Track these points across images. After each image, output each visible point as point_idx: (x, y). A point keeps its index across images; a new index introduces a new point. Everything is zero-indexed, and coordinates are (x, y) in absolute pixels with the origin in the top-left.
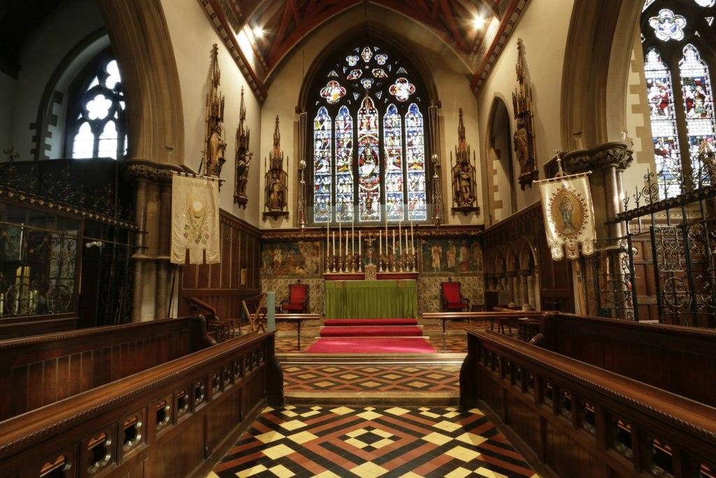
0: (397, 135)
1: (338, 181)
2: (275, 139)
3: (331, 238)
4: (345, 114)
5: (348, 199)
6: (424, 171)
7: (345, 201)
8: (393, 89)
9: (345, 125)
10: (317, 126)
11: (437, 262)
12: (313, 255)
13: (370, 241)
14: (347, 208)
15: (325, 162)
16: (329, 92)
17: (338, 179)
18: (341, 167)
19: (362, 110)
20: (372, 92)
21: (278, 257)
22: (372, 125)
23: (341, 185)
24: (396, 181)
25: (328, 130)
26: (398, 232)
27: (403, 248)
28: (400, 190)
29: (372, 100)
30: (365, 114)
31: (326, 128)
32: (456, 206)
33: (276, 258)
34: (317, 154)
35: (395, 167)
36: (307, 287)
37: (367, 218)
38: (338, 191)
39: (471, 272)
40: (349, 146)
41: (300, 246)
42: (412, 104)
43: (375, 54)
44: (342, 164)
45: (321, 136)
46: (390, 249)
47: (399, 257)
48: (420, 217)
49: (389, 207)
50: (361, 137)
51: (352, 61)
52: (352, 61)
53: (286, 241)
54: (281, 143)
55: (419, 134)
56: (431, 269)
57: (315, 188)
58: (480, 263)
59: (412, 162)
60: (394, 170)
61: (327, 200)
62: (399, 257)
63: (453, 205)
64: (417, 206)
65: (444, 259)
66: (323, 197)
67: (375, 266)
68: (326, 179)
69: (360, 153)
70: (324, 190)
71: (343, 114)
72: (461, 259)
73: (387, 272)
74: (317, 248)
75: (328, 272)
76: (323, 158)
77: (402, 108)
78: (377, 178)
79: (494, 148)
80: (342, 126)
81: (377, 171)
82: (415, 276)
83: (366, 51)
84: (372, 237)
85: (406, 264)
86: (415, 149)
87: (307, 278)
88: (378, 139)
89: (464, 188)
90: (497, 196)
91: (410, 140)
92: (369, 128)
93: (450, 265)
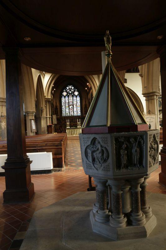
20: (71, 94)
52: (68, 88)
77: (76, 97)
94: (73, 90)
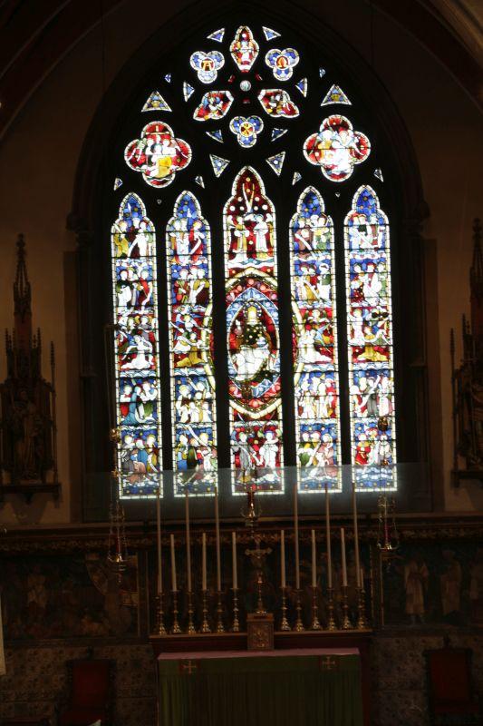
0: (324, 271)
1: (177, 391)
2: (16, 298)
3: (166, 548)
4: (189, 215)
5: (204, 438)
6: (391, 365)
7: (195, 443)
8: (314, 148)
9: (192, 243)
10: (119, 248)
14: (200, 461)
15: (141, 344)
16: (148, 152)
17: (177, 386)
18: (183, 356)
19: (234, 203)
20: (257, 155)
22: (261, 244)
23: (185, 401)
24: (322, 392)
26: (324, 531)
28: (333, 416)
29: (258, 177)
30: (241, 214)
31: (142, 252)
32: (462, 466)
33: (32, 597)
38: (178, 418)
40: (202, 299)
41: (89, 567)
42: (361, 189)
43: (265, 46)
44: (185, 349)
45: (131, 272)
46: (306, 570)
47: (323, 592)
48: (381, 483)
50: (232, 276)
51: (206, 66)
52: (206, 66)
54: (35, 307)
55: (381, 268)
60: (317, 363)
61: (151, 441)
63: (456, 464)
64: (373, 457)
68: (146, 386)
69: (231, 318)
70: (141, 415)
71: (185, 214)
76: (137, 332)
77: (338, 201)
78: (275, 385)
80: (183, 247)
81: (274, 365)
83: (241, 39)
84: (264, 545)
86: (369, 308)
88: (275, 283)
91: (356, 285)
92: (252, 252)
94: (282, 105)
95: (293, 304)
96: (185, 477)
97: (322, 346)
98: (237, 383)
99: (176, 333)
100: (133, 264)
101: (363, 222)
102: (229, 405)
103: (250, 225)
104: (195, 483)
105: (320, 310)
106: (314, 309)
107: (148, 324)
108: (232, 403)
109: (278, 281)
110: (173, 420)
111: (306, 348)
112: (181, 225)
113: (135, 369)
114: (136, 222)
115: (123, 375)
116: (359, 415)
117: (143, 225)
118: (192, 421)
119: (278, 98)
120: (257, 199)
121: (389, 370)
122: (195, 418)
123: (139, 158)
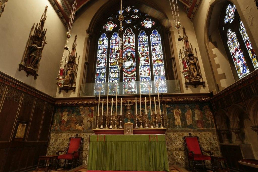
1: (110, 71)
3: (101, 104)
4: (116, 36)
5: (116, 81)
8: (143, 24)
9: (116, 41)
11: (178, 121)
12: (89, 116)
13: (129, 105)
16: (108, 26)
18: (112, 63)
19: (126, 34)
21: (65, 118)
22: (131, 41)
24: (146, 70)
25: (106, 44)
26: (149, 99)
27: (152, 111)
28: (149, 75)
30: (127, 36)
31: (105, 43)
32: (188, 81)
34: (99, 57)
35: (145, 62)
36: (82, 140)
37: (128, 92)
38: (110, 76)
39: (205, 128)
40: (117, 52)
42: (153, 30)
44: (113, 62)
45: (102, 47)
46: (143, 111)
49: (142, 85)
50: (124, 47)
53: (72, 106)
54: (77, 49)
55: (159, 44)
56: (175, 126)
57: (96, 75)
58: (212, 121)
59: (156, 59)
60: (145, 64)
62: (150, 117)
64: (160, 84)
65: (183, 119)
66: (100, 80)
67: (132, 124)
68: (103, 70)
69: (124, 55)
71: (115, 36)
72: (197, 119)
73: (141, 128)
74: (92, 111)
75: (97, 129)
76: (102, 58)
77: (148, 32)
78: (134, 69)
79: (212, 42)
80: (114, 42)
81: (134, 64)
82: (162, 132)
83: (128, 8)
85: (155, 122)
86: (157, 52)
87: (83, 132)
88: (134, 48)
89: (192, 70)
90: (220, 71)
91: (153, 48)
92: (129, 42)
93: (189, 123)
95: (139, 52)
96: (111, 90)
97: (146, 60)
98: (125, 68)
99: (111, 58)
100: (103, 46)
101: (154, 36)
102: (123, 73)
103: (129, 38)
104: (113, 91)
105: (145, 53)
106: (144, 53)
107: (105, 57)
108: (124, 73)
109: (135, 48)
110: (109, 77)
111: (142, 61)
112: (114, 38)
113: (101, 66)
114: (104, 38)
115: (98, 67)
116: (156, 75)
117: (106, 38)
118: (114, 77)
119: (135, 16)
120: (131, 33)
121: (163, 65)
122: (114, 76)
123: (106, 27)
